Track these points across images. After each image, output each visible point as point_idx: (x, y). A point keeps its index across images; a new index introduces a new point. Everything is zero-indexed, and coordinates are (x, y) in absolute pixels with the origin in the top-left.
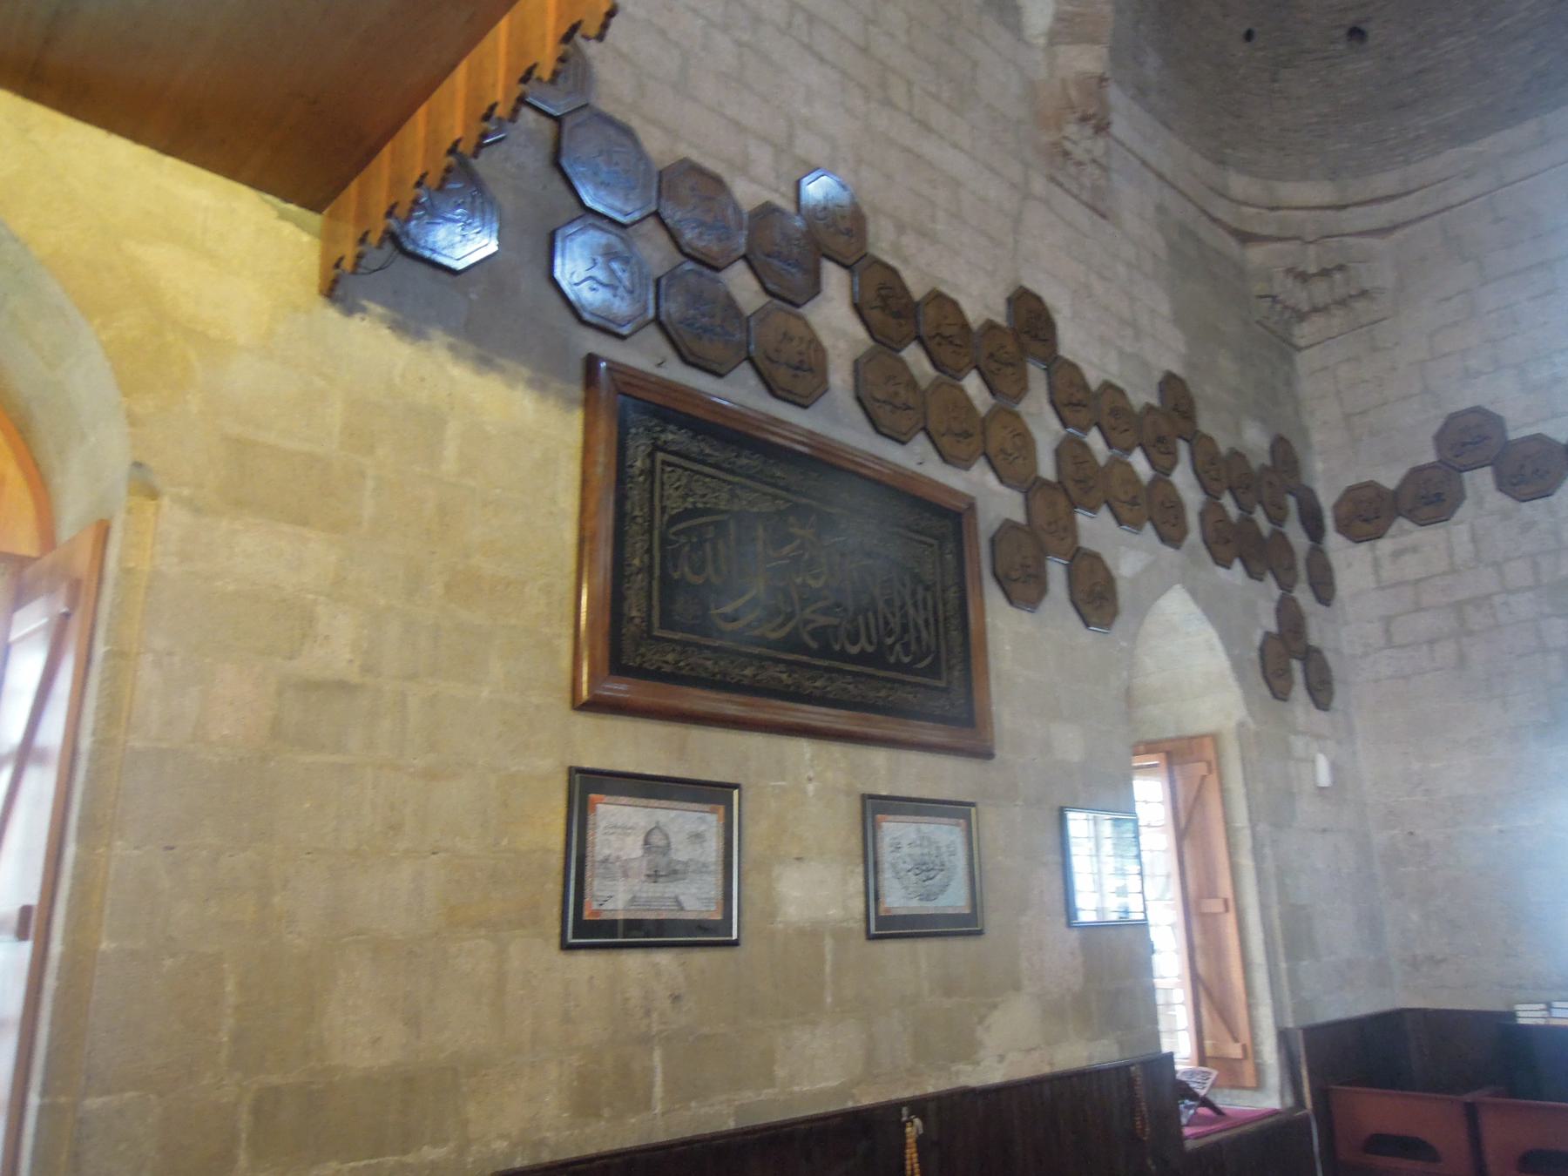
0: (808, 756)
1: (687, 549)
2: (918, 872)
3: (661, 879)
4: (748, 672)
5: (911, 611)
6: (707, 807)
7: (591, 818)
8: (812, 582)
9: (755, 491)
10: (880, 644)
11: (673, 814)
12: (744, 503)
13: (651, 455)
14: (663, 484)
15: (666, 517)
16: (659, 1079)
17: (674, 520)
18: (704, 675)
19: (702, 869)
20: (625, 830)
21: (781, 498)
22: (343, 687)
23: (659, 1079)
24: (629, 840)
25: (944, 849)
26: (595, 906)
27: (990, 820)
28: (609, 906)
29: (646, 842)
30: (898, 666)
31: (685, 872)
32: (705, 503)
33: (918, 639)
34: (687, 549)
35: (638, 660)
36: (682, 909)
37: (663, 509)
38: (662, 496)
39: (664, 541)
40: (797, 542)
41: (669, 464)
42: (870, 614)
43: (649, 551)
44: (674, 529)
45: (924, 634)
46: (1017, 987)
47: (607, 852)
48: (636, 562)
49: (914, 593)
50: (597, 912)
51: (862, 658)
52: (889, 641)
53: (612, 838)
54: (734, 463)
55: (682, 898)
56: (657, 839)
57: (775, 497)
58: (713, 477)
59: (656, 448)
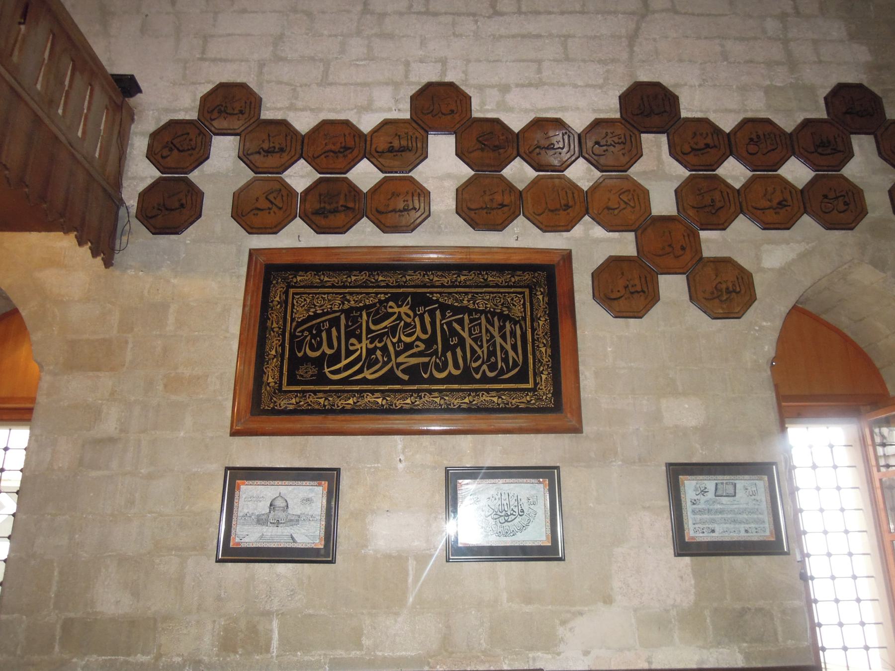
0: (400, 447)
1: (308, 338)
2: (497, 516)
3: (281, 525)
4: (351, 401)
5: (499, 340)
6: (316, 483)
7: (237, 493)
8: (403, 338)
9: (361, 293)
10: (467, 368)
11: (290, 488)
12: (352, 302)
13: (286, 293)
14: (293, 305)
15: (294, 324)
16: (276, 636)
17: (300, 324)
18: (317, 407)
19: (310, 518)
20: (258, 499)
21: (381, 293)
22: (111, 440)
23: (276, 636)
24: (261, 504)
25: (524, 501)
26: (237, 540)
27: (569, 480)
28: (246, 540)
29: (271, 505)
30: (485, 379)
31: (298, 521)
32: (323, 310)
33: (505, 360)
34: (308, 338)
35: (271, 406)
36: (294, 541)
37: (293, 320)
38: (292, 312)
39: (293, 336)
40: (395, 316)
41: (297, 294)
42: (459, 350)
43: (283, 345)
44: (299, 330)
45: (511, 353)
46: (608, 600)
47: (246, 511)
48: (273, 352)
49: (502, 328)
50: (239, 544)
51: (450, 379)
52: (474, 365)
53: (250, 503)
54: (346, 281)
55: (294, 536)
56: (280, 503)
57: (377, 294)
58: (328, 293)
59: (289, 286)
